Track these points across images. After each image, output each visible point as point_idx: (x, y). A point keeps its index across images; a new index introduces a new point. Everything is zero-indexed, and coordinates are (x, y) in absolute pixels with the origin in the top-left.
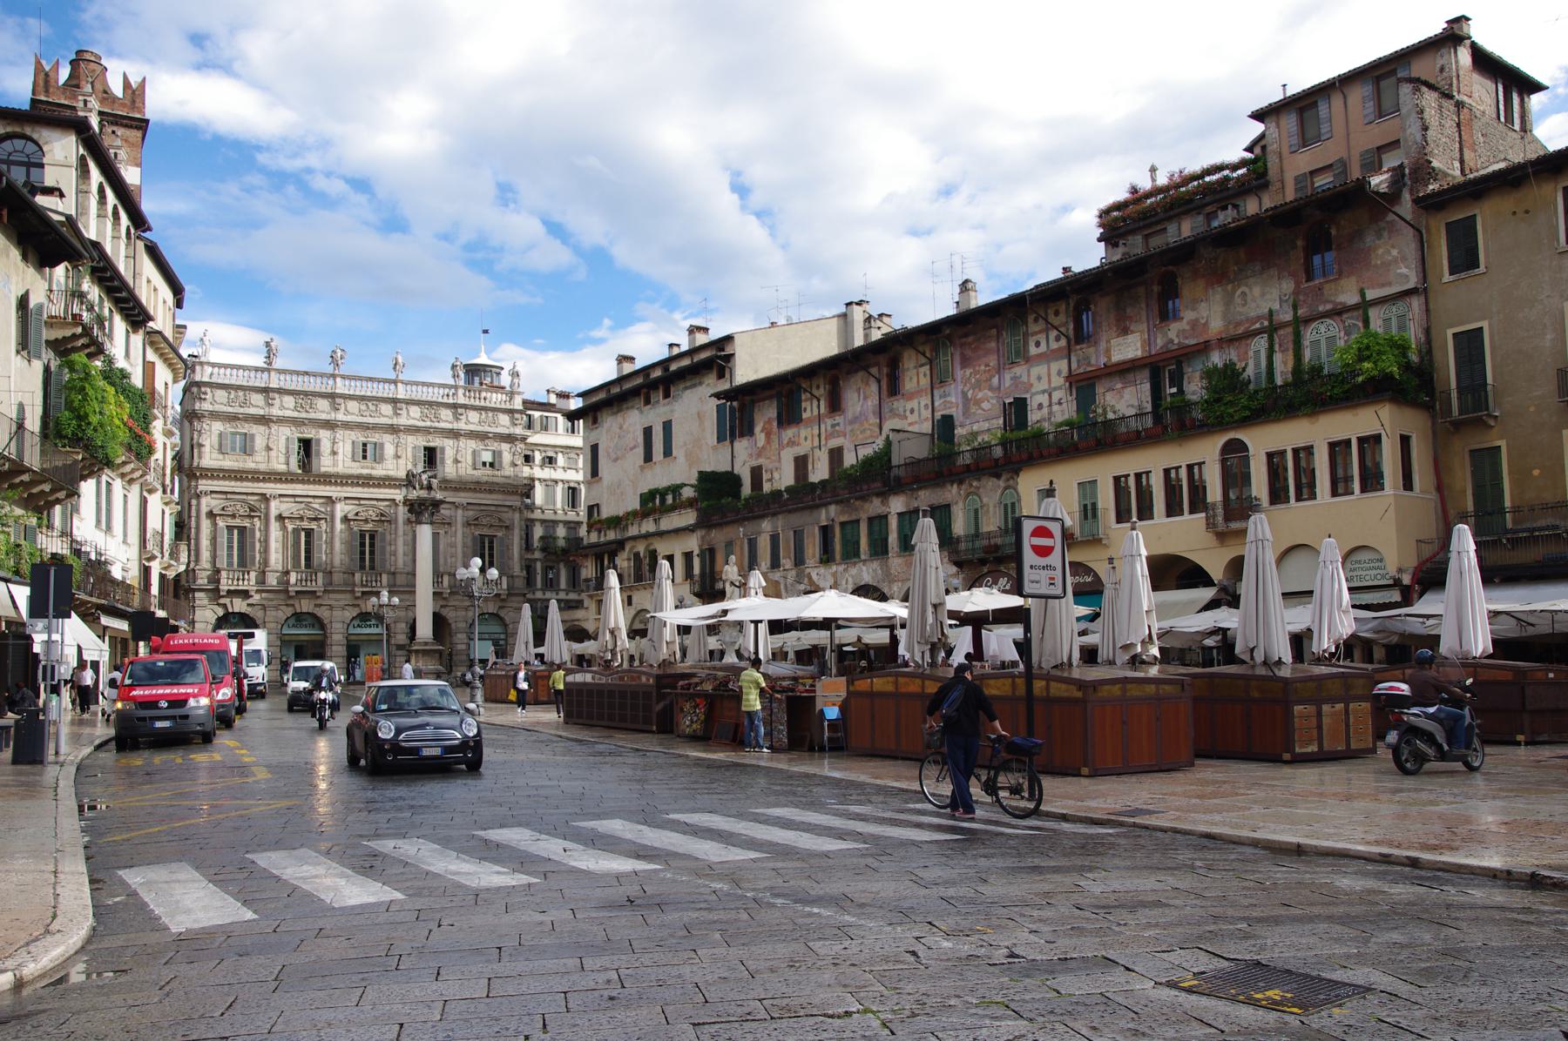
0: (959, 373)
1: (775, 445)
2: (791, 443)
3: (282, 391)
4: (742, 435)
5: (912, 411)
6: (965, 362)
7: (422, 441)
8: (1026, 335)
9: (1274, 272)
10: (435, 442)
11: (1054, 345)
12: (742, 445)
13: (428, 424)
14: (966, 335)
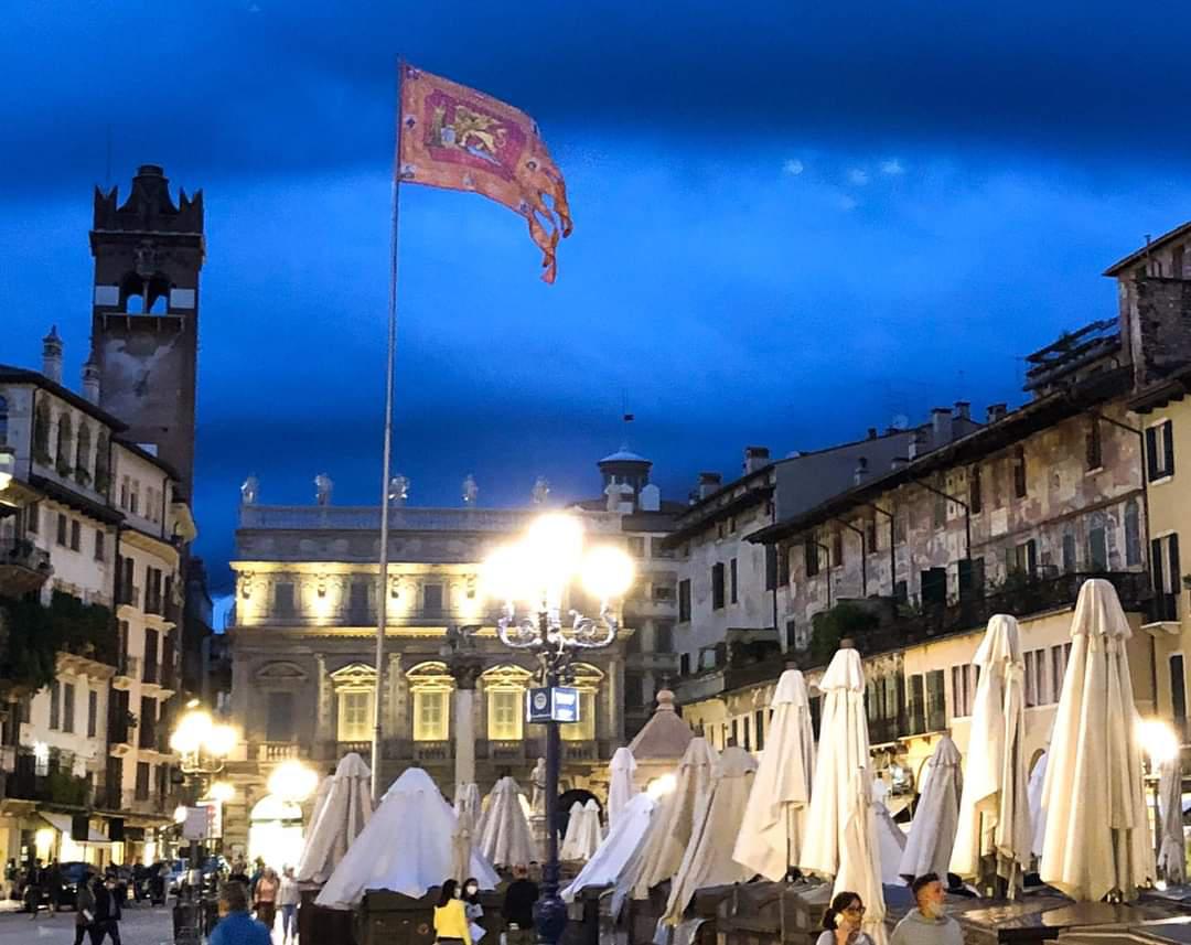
2: (813, 598)
4: (782, 585)
9: (1072, 457)
12: (781, 594)
14: (912, 493)
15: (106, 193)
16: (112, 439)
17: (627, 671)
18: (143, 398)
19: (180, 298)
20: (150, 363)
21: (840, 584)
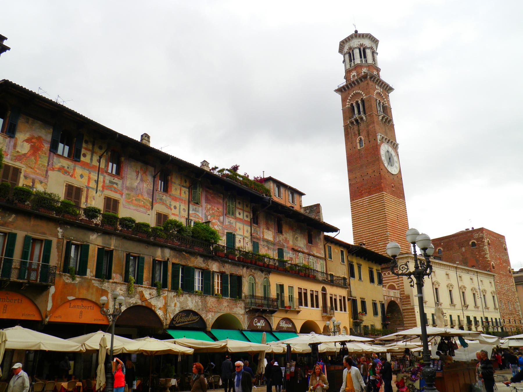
1: (43, 161)
6: (208, 201)
11: (246, 219)
21: (115, 186)
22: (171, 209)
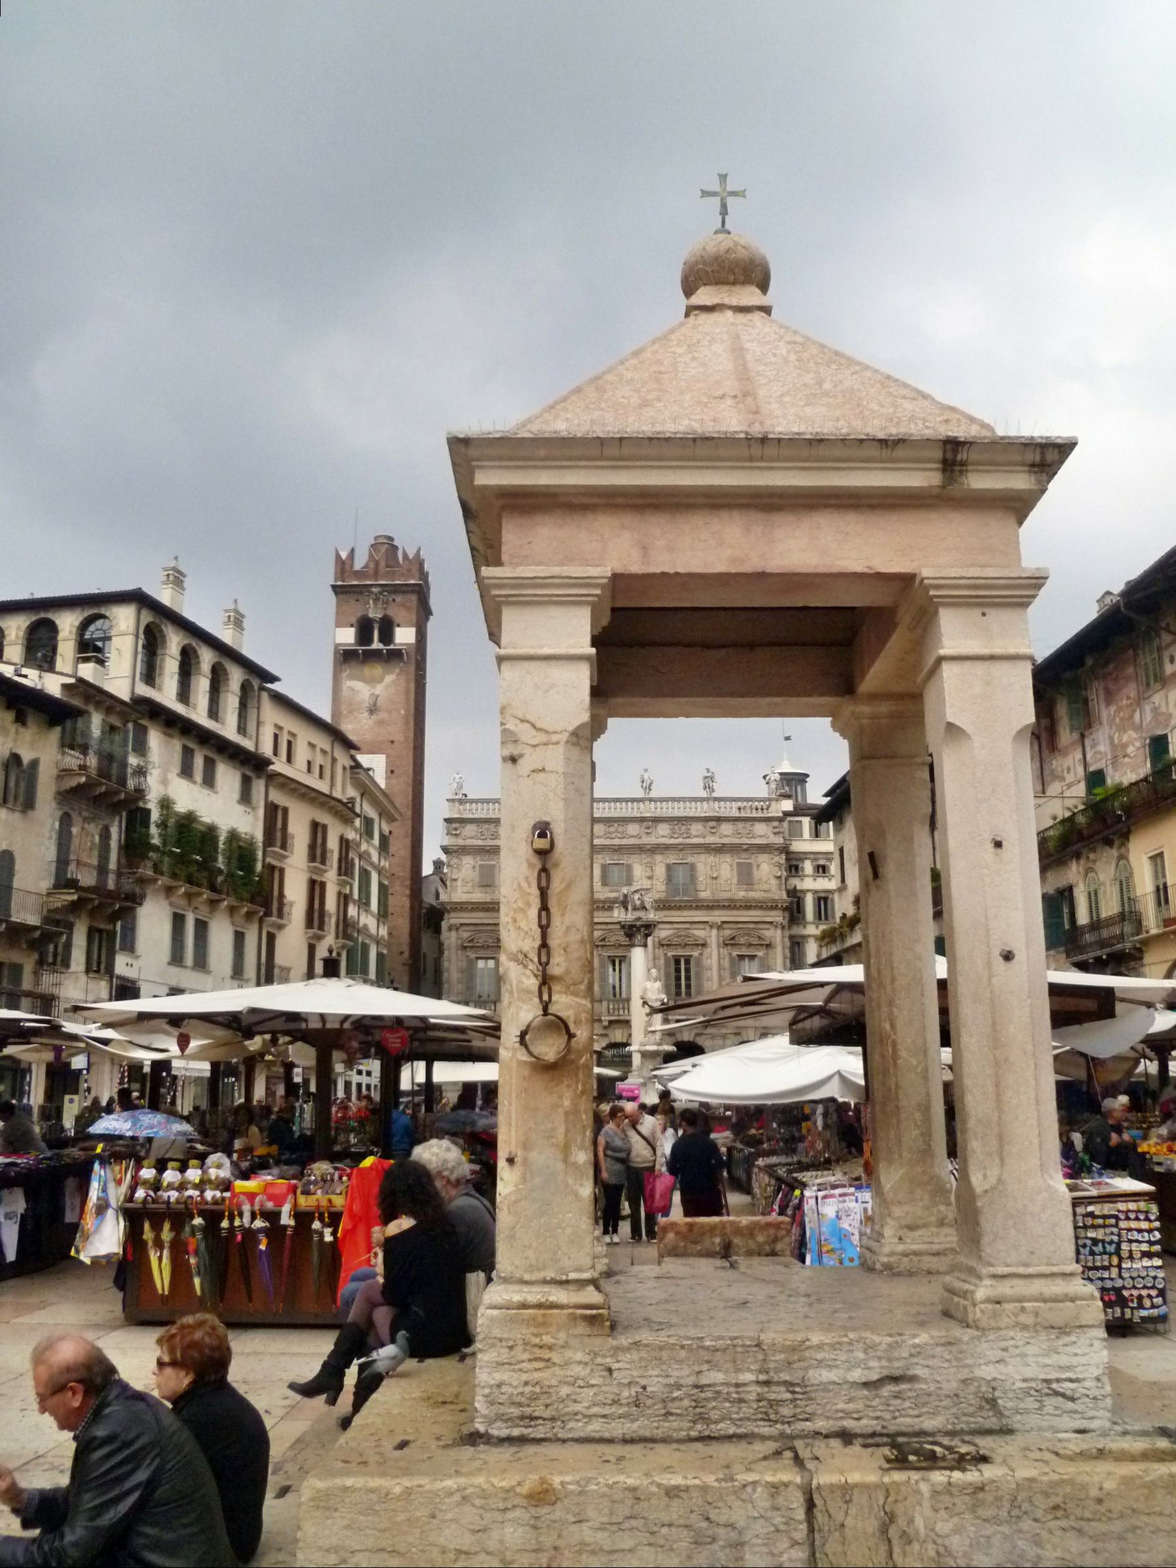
0: (1104, 714)
3: (657, 820)
5: (1069, 770)
6: (1110, 697)
7: (672, 859)
8: (1160, 649)
10: (690, 859)
13: (680, 840)
14: (1107, 664)
15: (344, 555)
16: (262, 689)
17: (791, 937)
18: (374, 717)
19: (404, 636)
20: (379, 689)
22: (1063, 779)
